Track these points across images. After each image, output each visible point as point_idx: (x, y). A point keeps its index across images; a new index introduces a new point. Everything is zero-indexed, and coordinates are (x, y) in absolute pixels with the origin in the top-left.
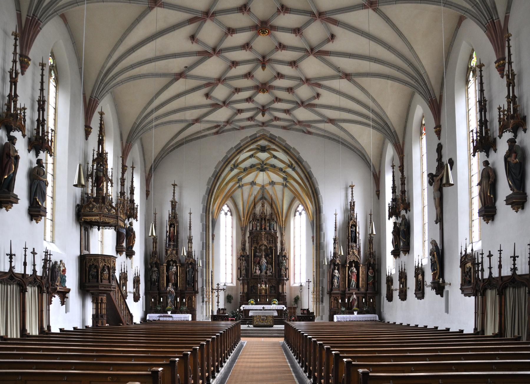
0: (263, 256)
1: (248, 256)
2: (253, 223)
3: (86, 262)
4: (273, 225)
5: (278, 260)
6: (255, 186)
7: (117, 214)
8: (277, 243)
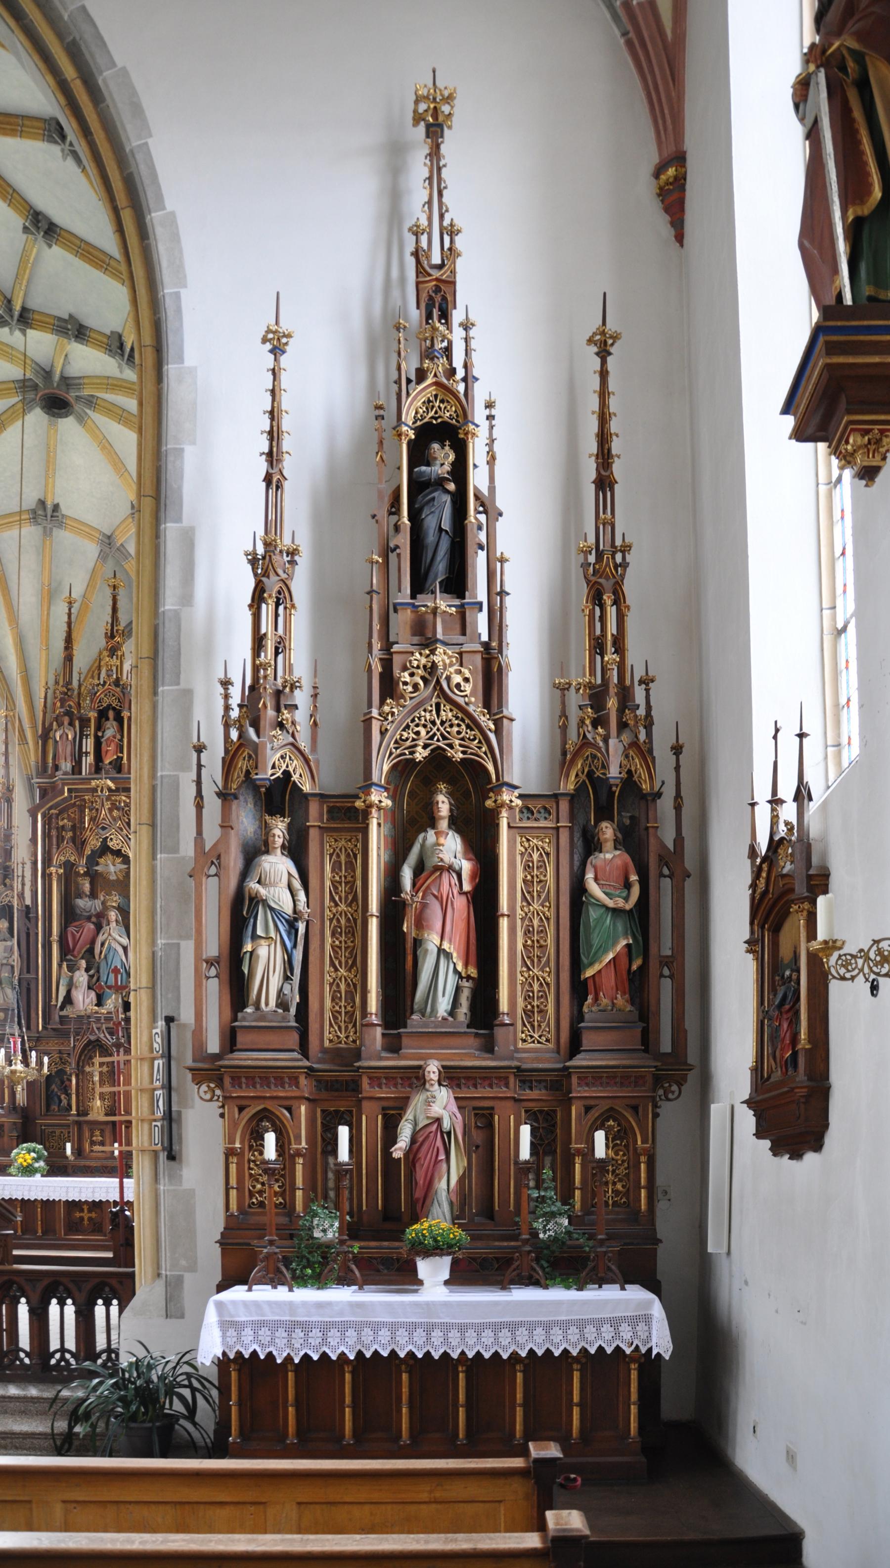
1: (28, 912)
6: (64, 537)
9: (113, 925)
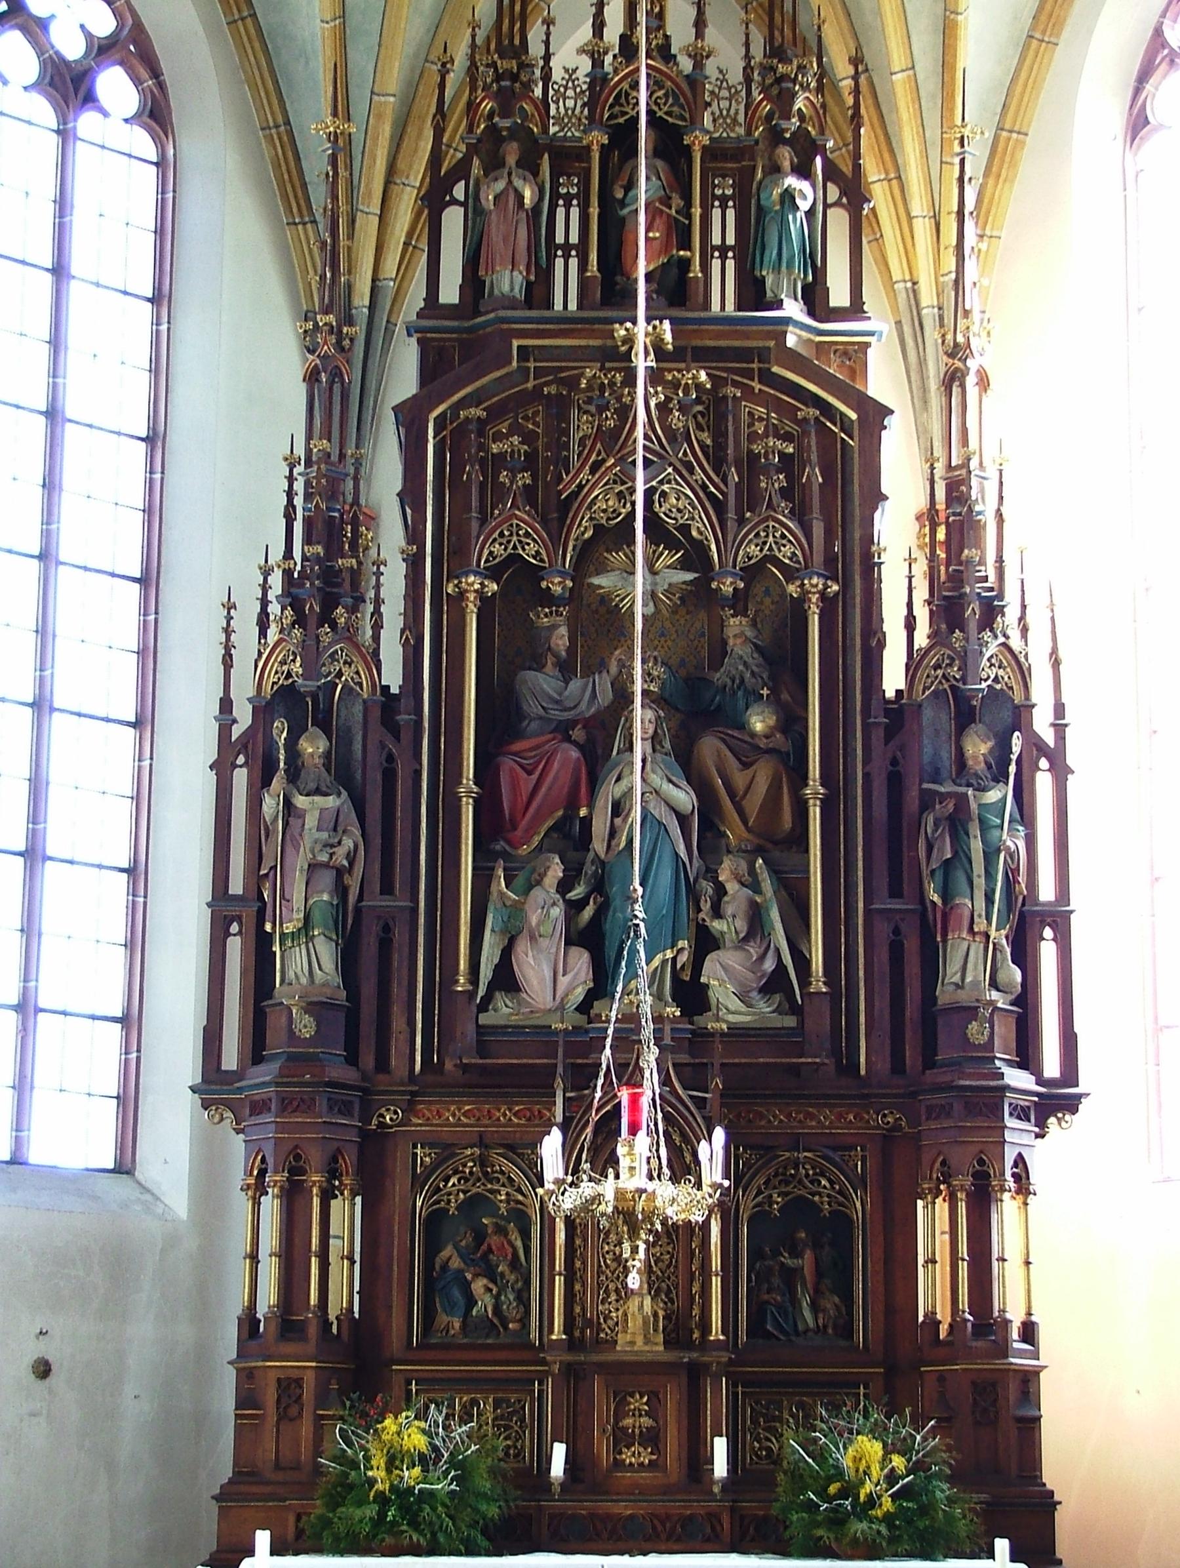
4: (796, 223)
5: (895, 781)
8: (876, 497)
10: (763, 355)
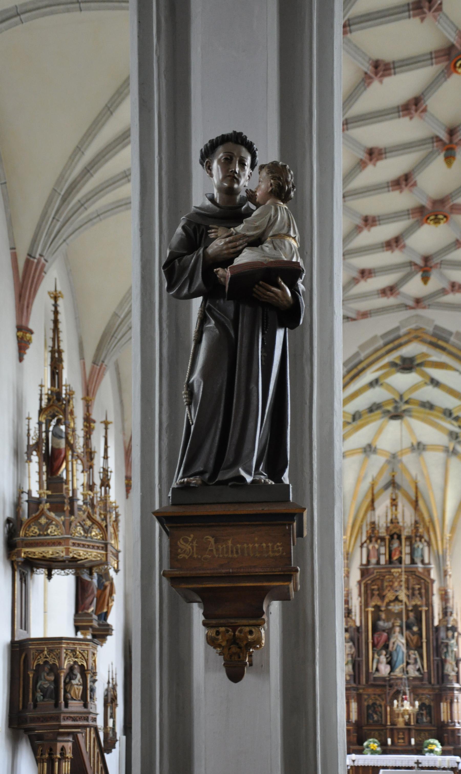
0: (397, 629)
1: (358, 629)
2: (370, 547)
3: (26, 657)
5: (437, 639)
7: (105, 538)
8: (433, 594)
9: (397, 634)
10: (415, 572)
